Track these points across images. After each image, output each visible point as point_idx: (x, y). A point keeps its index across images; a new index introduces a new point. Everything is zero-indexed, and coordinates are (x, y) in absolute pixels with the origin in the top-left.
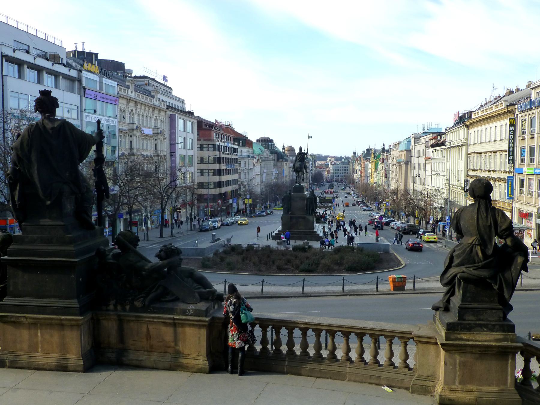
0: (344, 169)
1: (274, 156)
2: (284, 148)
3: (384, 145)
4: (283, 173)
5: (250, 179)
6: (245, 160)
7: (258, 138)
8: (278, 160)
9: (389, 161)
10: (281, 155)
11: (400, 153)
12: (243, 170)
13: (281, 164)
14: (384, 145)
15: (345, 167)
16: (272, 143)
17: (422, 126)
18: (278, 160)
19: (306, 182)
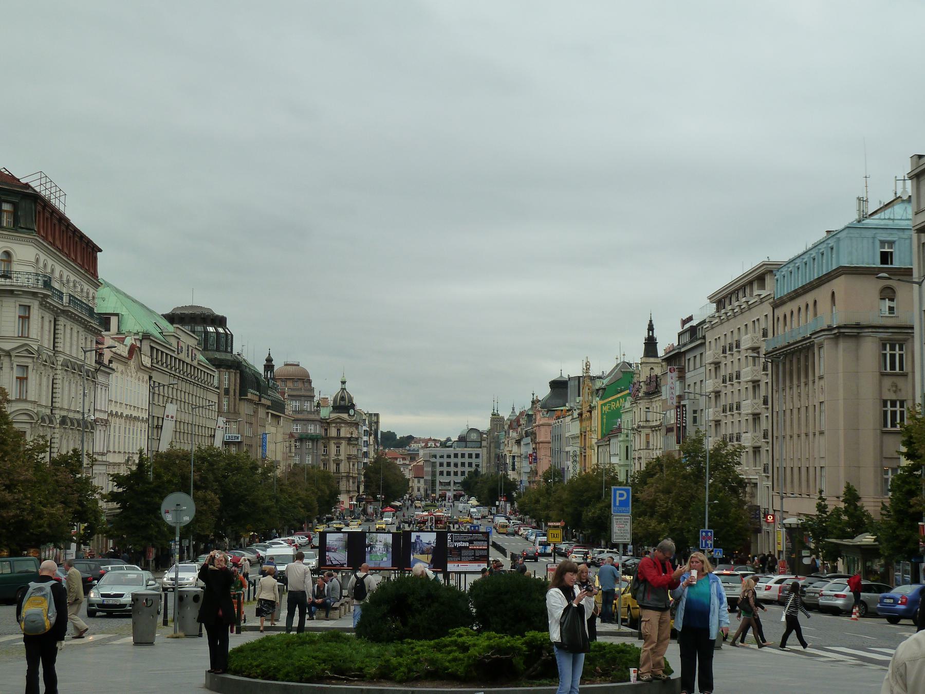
0: (467, 460)
1: (227, 379)
2: (269, 366)
3: (651, 328)
4: (263, 446)
5: (64, 413)
6: (26, 301)
7: (168, 311)
8: (243, 392)
9: (688, 375)
10: (257, 379)
11: (780, 312)
12: (8, 354)
13: (256, 412)
14: (651, 328)
15: (470, 456)
16: (221, 330)
17: (855, 203)
18: (243, 392)
19: (348, 492)
